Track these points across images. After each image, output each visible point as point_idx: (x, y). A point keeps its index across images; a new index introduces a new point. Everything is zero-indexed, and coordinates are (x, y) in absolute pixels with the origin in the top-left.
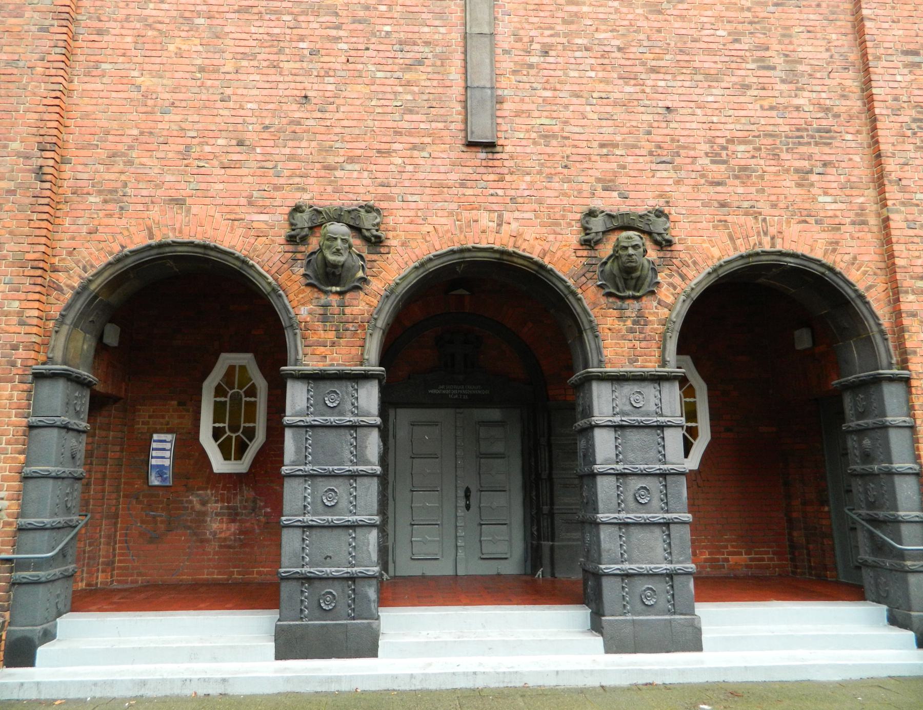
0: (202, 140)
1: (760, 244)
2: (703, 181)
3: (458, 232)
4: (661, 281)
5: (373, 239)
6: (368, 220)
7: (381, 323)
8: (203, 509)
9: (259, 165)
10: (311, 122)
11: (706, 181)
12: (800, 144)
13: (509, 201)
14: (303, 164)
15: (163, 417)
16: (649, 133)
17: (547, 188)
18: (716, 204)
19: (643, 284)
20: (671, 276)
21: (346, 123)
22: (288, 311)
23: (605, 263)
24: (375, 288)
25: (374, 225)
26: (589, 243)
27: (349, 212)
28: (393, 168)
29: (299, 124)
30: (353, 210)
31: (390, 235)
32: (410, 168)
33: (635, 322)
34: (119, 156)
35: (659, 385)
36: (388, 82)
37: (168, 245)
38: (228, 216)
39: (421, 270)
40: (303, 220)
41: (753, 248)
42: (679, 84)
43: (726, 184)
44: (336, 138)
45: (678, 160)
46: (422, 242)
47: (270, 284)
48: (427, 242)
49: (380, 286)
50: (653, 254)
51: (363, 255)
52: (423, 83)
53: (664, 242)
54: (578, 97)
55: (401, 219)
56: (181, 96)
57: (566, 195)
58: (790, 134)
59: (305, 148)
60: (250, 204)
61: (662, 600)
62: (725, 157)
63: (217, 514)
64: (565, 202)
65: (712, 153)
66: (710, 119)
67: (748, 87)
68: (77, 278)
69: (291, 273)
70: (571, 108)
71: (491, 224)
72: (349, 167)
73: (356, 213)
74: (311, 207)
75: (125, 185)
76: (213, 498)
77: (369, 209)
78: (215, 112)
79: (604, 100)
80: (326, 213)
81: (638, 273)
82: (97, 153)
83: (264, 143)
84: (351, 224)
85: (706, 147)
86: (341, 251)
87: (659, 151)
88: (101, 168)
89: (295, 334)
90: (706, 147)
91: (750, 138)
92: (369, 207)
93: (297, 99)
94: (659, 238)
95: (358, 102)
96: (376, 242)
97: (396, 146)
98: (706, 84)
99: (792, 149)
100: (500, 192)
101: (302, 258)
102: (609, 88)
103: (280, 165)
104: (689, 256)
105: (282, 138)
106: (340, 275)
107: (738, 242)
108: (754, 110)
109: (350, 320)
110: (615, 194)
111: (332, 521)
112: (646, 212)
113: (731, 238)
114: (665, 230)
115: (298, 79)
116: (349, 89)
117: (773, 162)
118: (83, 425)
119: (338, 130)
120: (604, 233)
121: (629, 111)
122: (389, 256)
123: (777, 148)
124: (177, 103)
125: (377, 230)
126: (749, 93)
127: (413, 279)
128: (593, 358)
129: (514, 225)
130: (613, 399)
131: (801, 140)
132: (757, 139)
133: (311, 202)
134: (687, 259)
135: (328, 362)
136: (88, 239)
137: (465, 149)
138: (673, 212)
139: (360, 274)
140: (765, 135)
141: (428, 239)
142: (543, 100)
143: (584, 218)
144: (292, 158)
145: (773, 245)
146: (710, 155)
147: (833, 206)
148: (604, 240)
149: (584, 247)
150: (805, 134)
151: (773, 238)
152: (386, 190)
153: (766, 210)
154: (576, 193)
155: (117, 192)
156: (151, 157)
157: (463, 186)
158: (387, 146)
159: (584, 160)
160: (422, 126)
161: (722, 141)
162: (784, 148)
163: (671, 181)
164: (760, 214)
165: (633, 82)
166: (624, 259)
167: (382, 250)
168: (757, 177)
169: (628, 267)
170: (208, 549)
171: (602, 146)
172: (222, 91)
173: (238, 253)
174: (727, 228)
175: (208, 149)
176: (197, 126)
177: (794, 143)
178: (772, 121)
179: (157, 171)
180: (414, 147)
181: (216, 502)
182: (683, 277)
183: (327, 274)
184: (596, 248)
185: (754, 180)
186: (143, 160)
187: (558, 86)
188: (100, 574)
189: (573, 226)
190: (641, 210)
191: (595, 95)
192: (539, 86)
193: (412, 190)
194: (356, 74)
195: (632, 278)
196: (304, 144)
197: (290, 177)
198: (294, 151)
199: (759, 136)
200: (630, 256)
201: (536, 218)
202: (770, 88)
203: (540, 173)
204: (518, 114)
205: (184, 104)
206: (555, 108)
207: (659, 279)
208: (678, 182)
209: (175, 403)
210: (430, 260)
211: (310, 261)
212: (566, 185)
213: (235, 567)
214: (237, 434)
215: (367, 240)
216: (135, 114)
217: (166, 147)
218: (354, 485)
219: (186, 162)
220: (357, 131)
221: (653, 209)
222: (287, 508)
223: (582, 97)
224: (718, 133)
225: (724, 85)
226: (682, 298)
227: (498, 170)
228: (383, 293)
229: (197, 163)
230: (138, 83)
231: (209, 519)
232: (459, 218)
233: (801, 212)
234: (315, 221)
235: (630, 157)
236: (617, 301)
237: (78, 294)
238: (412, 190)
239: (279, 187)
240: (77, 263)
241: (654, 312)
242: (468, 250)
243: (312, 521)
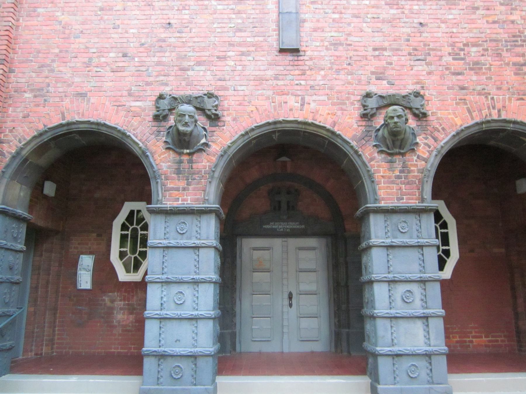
0: (99, 54)
1: (490, 115)
2: (447, 72)
3: (272, 110)
4: (419, 142)
5: (213, 116)
6: (209, 104)
7: (217, 174)
8: (112, 305)
9: (136, 69)
10: (173, 40)
11: (450, 72)
12: (516, 46)
13: (309, 88)
14: (166, 67)
15: (87, 244)
16: (408, 40)
17: (336, 79)
18: (458, 88)
19: (406, 144)
20: (426, 138)
21: (196, 40)
22: (152, 167)
23: (379, 130)
24: (214, 150)
25: (213, 107)
27: (196, 98)
28: (227, 68)
29: (164, 41)
30: (199, 97)
31: (225, 113)
32: (239, 68)
33: (401, 172)
34: (45, 67)
35: (419, 216)
36: (225, 12)
37: (74, 123)
38: (115, 104)
39: (246, 137)
40: (165, 104)
41: (486, 118)
42: (428, 7)
43: (464, 74)
44: (189, 49)
45: (429, 59)
46: (247, 118)
47: (140, 148)
48: (251, 117)
49: (218, 149)
50: (412, 123)
51: (206, 127)
52: (249, 12)
53: (421, 115)
54: (358, 17)
55: (233, 102)
56: (87, 27)
57: (349, 83)
58: (508, 39)
59: (168, 57)
60: (130, 95)
61: (423, 373)
62: (462, 56)
63: (121, 309)
64: (349, 88)
65: (453, 53)
66: (451, 30)
67: (477, 8)
68: (15, 147)
69: (156, 141)
70: (352, 25)
71: (296, 104)
72: (197, 68)
73: (201, 98)
74: (170, 95)
75: (48, 85)
76: (119, 298)
77: (210, 96)
78: (109, 36)
79: (376, 20)
80: (180, 99)
81: (402, 136)
82: (31, 65)
83: (140, 54)
84: (198, 106)
85: (450, 49)
86: (189, 124)
87: (416, 52)
88: (34, 75)
89: (157, 183)
90: (450, 49)
91: (480, 42)
92: (210, 94)
93: (164, 25)
94: (417, 112)
95: (205, 26)
98: (447, 7)
99: (510, 50)
100: (303, 83)
101: (164, 130)
102: (379, 11)
103: (151, 69)
104: (439, 124)
105: (152, 51)
106: (189, 141)
107: (474, 114)
108: (482, 24)
109: (196, 173)
110: (385, 82)
111: (180, 315)
112: (407, 94)
114: (422, 106)
115: (165, 12)
116: (199, 18)
117: (497, 59)
118: (21, 246)
119: (190, 44)
120: (377, 109)
121: (394, 26)
122: (225, 128)
123: (500, 49)
124: (84, 31)
125: (216, 110)
126: (478, 12)
127: (240, 143)
128: (370, 196)
129: (313, 105)
130: (386, 227)
131: (516, 43)
132: (485, 43)
133: (171, 93)
134: (437, 126)
135: (180, 202)
136: (23, 121)
137: (277, 54)
138: (427, 94)
139: (203, 141)
140: (491, 41)
141: (252, 115)
142: (333, 20)
143: (363, 99)
144: (159, 63)
145: (499, 115)
146: (452, 54)
148: (378, 114)
149: (363, 119)
150: (519, 39)
151: (499, 111)
152: (223, 83)
153: (493, 91)
154: (357, 82)
155: (43, 90)
156: (66, 66)
157: (276, 79)
158: (224, 54)
159: (362, 59)
160: (249, 40)
161: (461, 45)
162: (505, 49)
163: (424, 73)
164: (489, 94)
165: (395, 7)
166: (392, 125)
167: (219, 124)
168: (486, 69)
169: (395, 131)
170: (114, 332)
171: (375, 50)
172: (114, 22)
173: (119, 128)
174: (466, 104)
175: (103, 60)
176: (96, 46)
177: (511, 46)
178: (495, 31)
179: (69, 75)
180: (243, 54)
181: (121, 300)
182: (435, 139)
183: (180, 141)
184: (372, 119)
185: (484, 71)
186: (61, 68)
187: (343, 11)
188: (44, 348)
189: (355, 105)
190: (404, 92)
191: (369, 16)
192: (330, 11)
193: (241, 83)
194: (204, 7)
195: (398, 140)
196: (167, 54)
197: (157, 76)
198: (160, 60)
199: (486, 41)
200: (395, 123)
201: (328, 99)
202: (493, 8)
203: (331, 68)
204: (315, 30)
205: (89, 31)
206: (341, 25)
207: (418, 140)
208: (429, 73)
209: (95, 235)
210: (252, 130)
211: (169, 132)
212: (349, 77)
213: (132, 344)
214: (135, 256)
215: (209, 117)
216: (57, 39)
217: (76, 60)
218: (197, 289)
219: (88, 69)
220: (203, 45)
221: (412, 92)
222: (149, 305)
223: (360, 17)
224: (457, 40)
225: (460, 7)
226: (434, 153)
227: (301, 68)
228: (219, 153)
229: (96, 69)
230: (60, 20)
231: (115, 312)
232: (274, 101)
233: (518, 93)
234: (173, 105)
235: (395, 57)
236: (388, 156)
237: (14, 157)
238: (241, 83)
239: (149, 83)
240: (15, 137)
241: (415, 164)
242: (280, 122)
243: (166, 314)
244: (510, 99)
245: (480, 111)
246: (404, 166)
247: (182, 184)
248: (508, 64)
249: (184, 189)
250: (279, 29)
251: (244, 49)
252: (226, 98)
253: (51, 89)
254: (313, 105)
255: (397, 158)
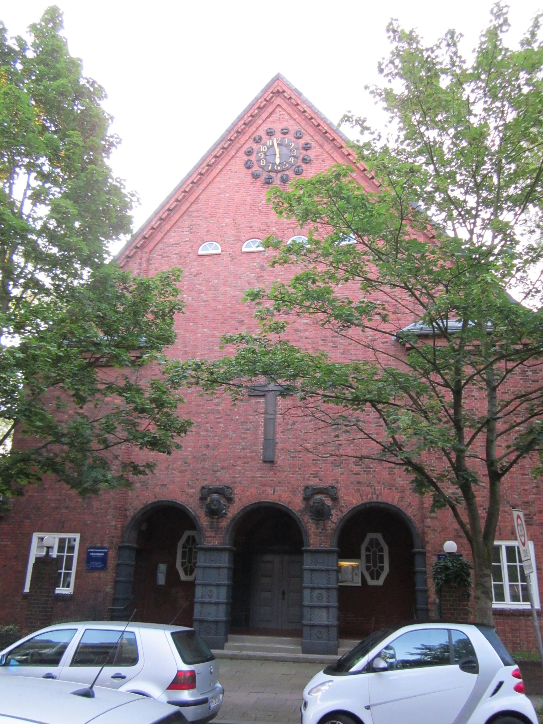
7: (230, 530)
26: (306, 499)
72: (222, 471)
77: (228, 487)
96: (230, 500)
97: (238, 463)
110: (317, 479)
113: (361, 496)
129: (279, 492)
139: (224, 511)
144: (203, 468)
145: (377, 499)
147: (403, 482)
152: (235, 479)
157: (261, 477)
160: (248, 455)
171: (313, 460)
175: (175, 466)
180: (245, 463)
182: (341, 512)
215: (227, 499)
244: (384, 489)
245: (367, 495)
246: (324, 526)
247: (213, 534)
248: (385, 468)
249: (214, 537)
250: (265, 449)
251: (246, 460)
252: (235, 488)
253: (149, 481)
254: (279, 492)
255: (321, 522)
